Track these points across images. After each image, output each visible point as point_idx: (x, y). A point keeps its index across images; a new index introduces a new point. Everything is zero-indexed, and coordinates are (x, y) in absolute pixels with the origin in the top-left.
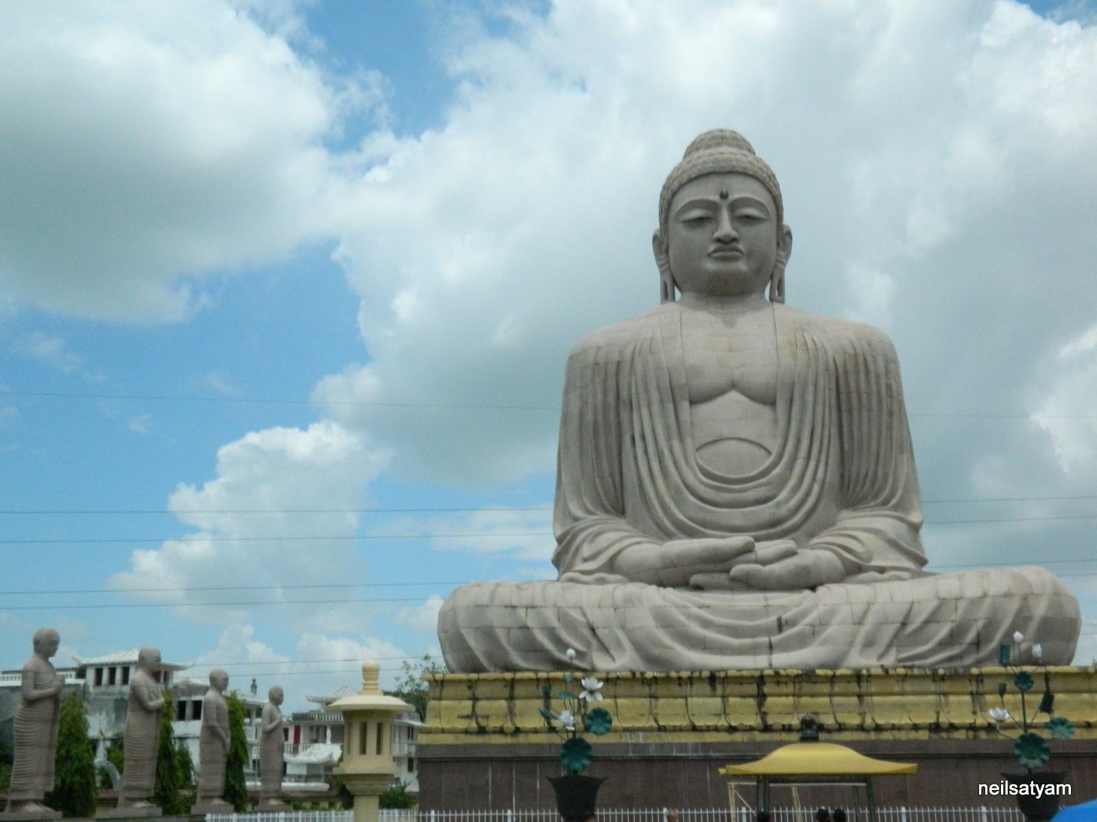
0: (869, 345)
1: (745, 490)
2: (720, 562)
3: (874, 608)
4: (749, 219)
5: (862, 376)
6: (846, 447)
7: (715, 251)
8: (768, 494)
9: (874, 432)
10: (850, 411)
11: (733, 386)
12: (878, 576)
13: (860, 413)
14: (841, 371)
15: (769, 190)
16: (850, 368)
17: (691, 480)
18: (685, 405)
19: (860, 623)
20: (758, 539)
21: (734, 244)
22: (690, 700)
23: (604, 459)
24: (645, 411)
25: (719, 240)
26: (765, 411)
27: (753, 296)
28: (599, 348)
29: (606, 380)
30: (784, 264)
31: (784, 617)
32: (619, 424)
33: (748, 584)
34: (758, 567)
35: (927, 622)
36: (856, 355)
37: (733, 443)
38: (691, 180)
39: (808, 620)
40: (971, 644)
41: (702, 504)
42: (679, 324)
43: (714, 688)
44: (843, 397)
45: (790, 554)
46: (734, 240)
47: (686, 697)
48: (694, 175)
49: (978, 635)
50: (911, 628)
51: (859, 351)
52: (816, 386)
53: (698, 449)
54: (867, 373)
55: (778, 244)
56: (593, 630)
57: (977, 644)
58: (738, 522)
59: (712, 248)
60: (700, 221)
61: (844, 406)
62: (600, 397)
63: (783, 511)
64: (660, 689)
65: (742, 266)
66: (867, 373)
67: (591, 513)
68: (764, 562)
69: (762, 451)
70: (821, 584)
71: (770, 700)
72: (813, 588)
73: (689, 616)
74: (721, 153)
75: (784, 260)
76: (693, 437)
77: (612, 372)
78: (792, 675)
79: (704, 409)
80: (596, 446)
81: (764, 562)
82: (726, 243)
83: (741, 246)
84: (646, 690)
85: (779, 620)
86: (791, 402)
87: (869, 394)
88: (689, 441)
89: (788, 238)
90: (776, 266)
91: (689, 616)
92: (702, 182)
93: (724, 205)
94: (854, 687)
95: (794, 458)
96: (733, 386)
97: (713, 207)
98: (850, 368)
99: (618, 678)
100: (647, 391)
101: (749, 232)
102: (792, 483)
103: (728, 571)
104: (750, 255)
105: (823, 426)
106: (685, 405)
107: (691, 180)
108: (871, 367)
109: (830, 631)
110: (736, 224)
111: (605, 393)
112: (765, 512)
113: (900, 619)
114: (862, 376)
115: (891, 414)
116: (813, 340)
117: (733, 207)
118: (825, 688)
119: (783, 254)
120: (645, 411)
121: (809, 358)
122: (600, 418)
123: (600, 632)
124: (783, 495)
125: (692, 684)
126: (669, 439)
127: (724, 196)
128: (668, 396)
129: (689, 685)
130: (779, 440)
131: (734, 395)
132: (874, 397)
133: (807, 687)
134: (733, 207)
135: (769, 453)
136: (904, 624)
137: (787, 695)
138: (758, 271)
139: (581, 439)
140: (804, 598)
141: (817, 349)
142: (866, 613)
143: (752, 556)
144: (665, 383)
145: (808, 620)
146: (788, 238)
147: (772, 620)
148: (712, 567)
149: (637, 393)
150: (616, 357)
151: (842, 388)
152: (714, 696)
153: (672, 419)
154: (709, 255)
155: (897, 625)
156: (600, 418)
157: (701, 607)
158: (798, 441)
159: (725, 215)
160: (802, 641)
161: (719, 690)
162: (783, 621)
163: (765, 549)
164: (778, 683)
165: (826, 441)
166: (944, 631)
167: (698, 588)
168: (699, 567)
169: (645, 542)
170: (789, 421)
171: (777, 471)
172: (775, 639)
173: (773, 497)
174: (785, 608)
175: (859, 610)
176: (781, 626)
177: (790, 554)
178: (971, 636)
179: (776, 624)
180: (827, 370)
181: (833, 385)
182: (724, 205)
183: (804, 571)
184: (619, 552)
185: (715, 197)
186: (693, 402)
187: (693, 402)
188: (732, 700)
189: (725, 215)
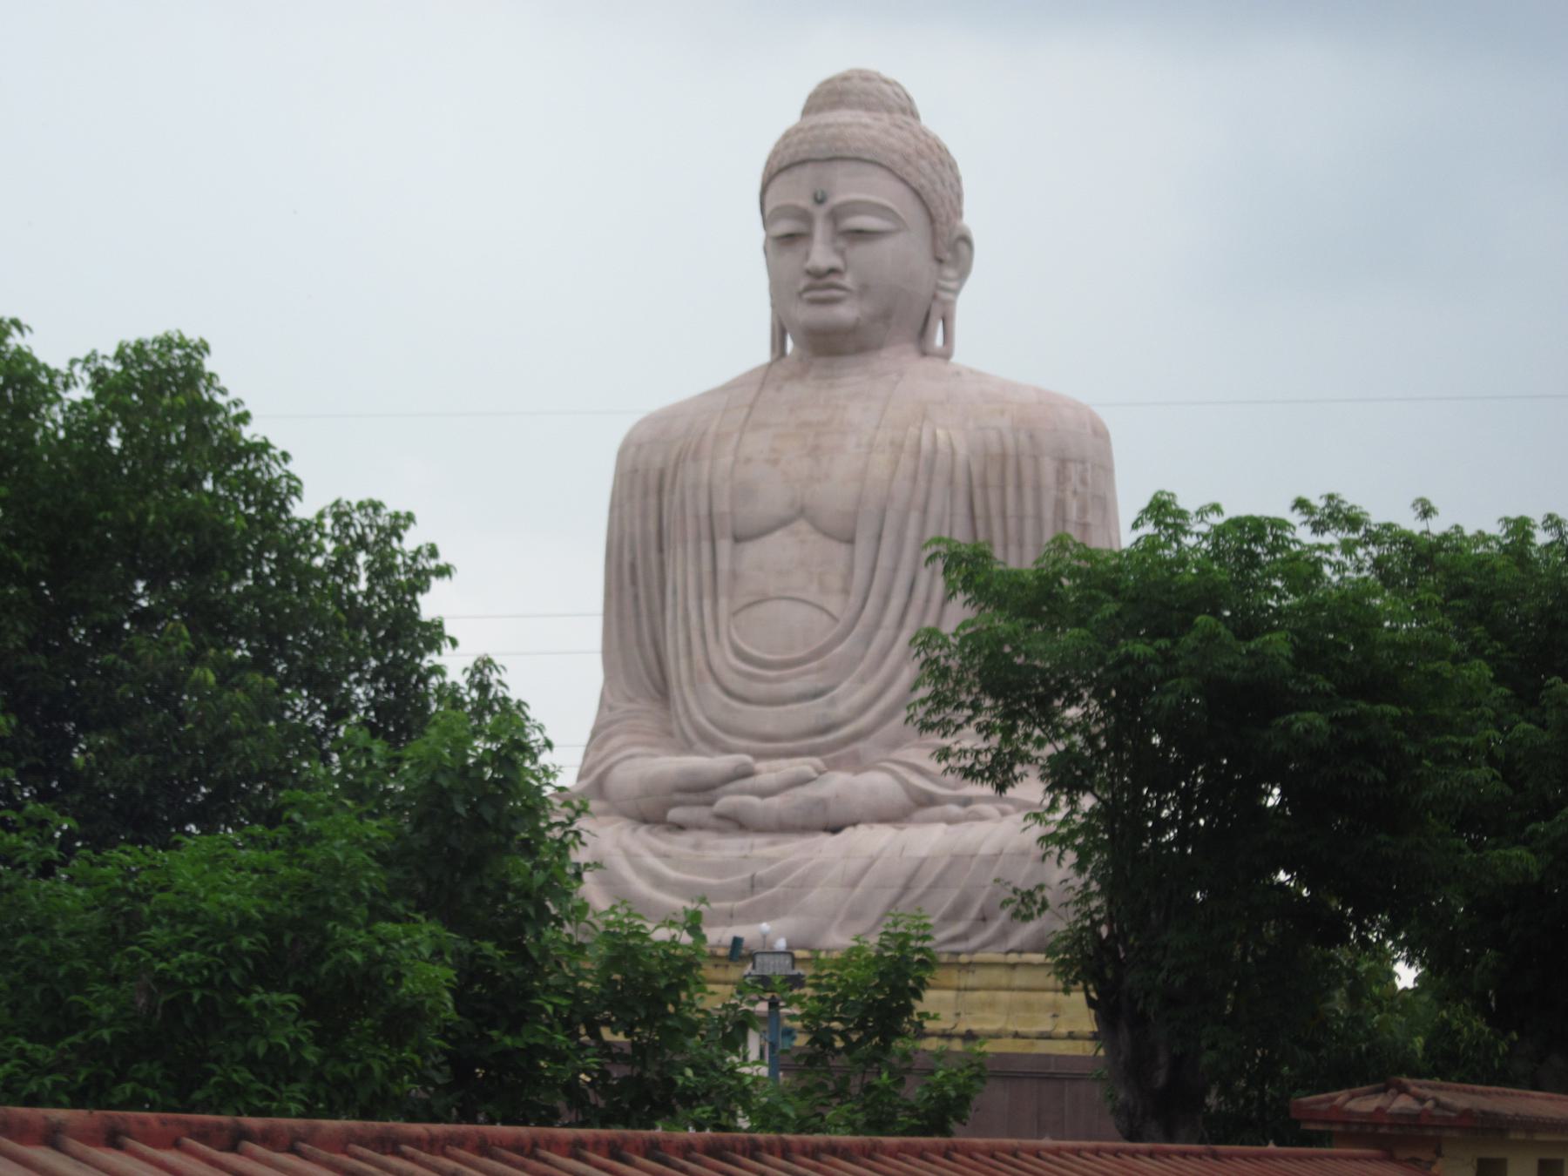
0: (1031, 437)
1: (779, 680)
2: (701, 789)
3: (878, 864)
5: (1011, 490)
7: (808, 289)
8: (821, 685)
12: (954, 809)
14: (976, 482)
15: (903, 181)
16: (993, 478)
17: (717, 662)
18: (724, 546)
19: (853, 884)
20: (759, 756)
21: (834, 279)
23: (644, 620)
24: (679, 550)
25: (808, 273)
26: (839, 551)
27: (884, 353)
28: (640, 446)
29: (645, 494)
30: (956, 292)
31: (762, 872)
33: (737, 823)
34: (755, 800)
35: (934, 886)
36: (1004, 456)
37: (784, 604)
38: (781, 170)
39: (785, 882)
40: (977, 920)
41: (726, 699)
42: (745, 410)
44: (980, 524)
45: (804, 781)
46: (833, 271)
48: (785, 163)
49: (982, 909)
50: (918, 892)
51: (1011, 451)
52: (925, 511)
53: (735, 614)
54: (1019, 487)
55: (940, 261)
57: (983, 919)
58: (769, 728)
59: (804, 282)
60: (789, 239)
62: (638, 523)
63: (841, 710)
65: (846, 313)
66: (1019, 487)
67: (630, 700)
68: (764, 793)
69: (825, 617)
70: (854, 824)
72: (835, 830)
73: (641, 870)
74: (828, 126)
75: (952, 285)
79: (752, 551)
80: (636, 597)
81: (764, 793)
82: (821, 277)
83: (848, 281)
86: (879, 537)
87: (1021, 519)
88: (723, 602)
89: (963, 247)
90: (935, 297)
91: (641, 870)
92: (797, 172)
93: (820, 212)
95: (877, 625)
96: (801, 512)
97: (805, 217)
98: (993, 478)
101: (861, 253)
102: (861, 668)
103: (710, 804)
104: (864, 290)
107: (781, 170)
108: (1028, 473)
109: (814, 896)
110: (841, 243)
111: (644, 517)
112: (810, 713)
113: (900, 881)
114: (1011, 490)
116: (935, 435)
117: (835, 216)
119: (950, 272)
120: (679, 550)
121: (893, 474)
122: (639, 556)
124: (845, 685)
126: (700, 598)
127: (819, 200)
128: (705, 531)
130: (854, 600)
131: (802, 526)
132: (1029, 525)
134: (835, 216)
135: (835, 619)
136: (907, 888)
137: (726, 983)
138: (885, 316)
139: (621, 588)
140: (827, 844)
141: (935, 450)
142: (864, 871)
143: (747, 783)
144: (703, 511)
145: (785, 882)
146: (963, 247)
147: (737, 879)
148: (693, 797)
150: (657, 461)
151: (979, 510)
153: (706, 566)
155: (895, 891)
156: (639, 556)
157: (664, 856)
158: (886, 598)
159: (821, 230)
160: (772, 910)
163: (770, 772)
166: (949, 898)
167: (680, 827)
168: (678, 797)
169: (642, 755)
170: (873, 570)
171: (839, 649)
173: (832, 688)
174: (770, 861)
175: (855, 865)
176: (754, 884)
177: (804, 781)
178: (974, 912)
180: (951, 482)
182: (820, 212)
183: (822, 803)
184: (610, 768)
185: (805, 202)
186: (738, 539)
187: (738, 539)
189: (821, 230)
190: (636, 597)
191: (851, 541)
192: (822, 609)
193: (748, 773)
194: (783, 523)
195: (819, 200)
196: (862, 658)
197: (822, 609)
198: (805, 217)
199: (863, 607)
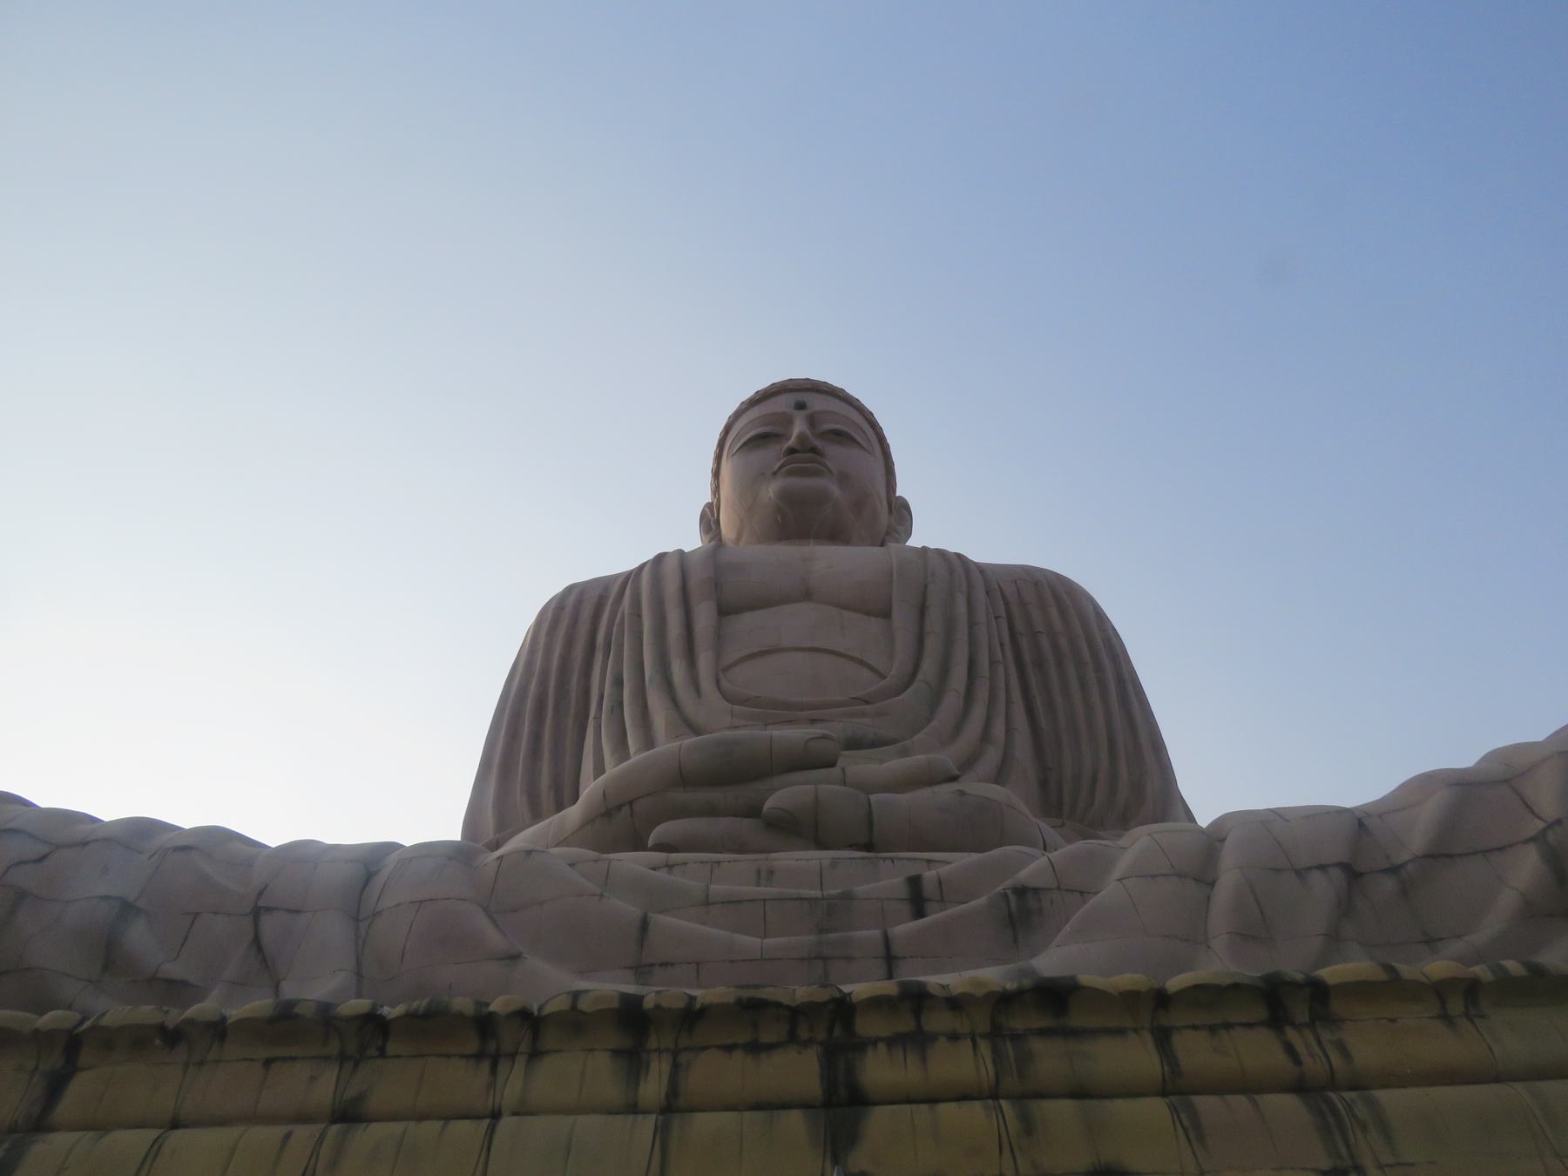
4: (839, 436)
6: (1044, 722)
7: (781, 467)
9: (1096, 698)
10: (1040, 665)
11: (807, 595)
13: (1060, 665)
22: (507, 1122)
25: (792, 451)
32: (586, 692)
35: (1439, 855)
43: (632, 1060)
44: (1025, 643)
46: (814, 450)
47: (496, 1115)
55: (890, 511)
56: (257, 913)
61: (1027, 657)
64: (390, 1081)
68: (868, 788)
71: (879, 1120)
76: (718, 652)
77: (586, 613)
78: (980, 993)
84: (324, 1087)
85: (915, 883)
86: (922, 610)
88: (704, 660)
94: (1257, 1050)
99: (218, 1029)
100: (638, 615)
105: (992, 663)
106: (704, 615)
115: (1121, 681)
118: (1134, 1056)
123: (268, 924)
125: (535, 1054)
129: (521, 1061)
133: (1050, 1059)
134: (812, 421)
149: (622, 623)
151: (1020, 625)
152: (633, 1109)
154: (775, 474)
161: (653, 1088)
162: (929, 888)
164: (919, 1041)
165: (1002, 685)
172: (904, 929)
176: (917, 899)
179: (903, 892)
181: (1003, 613)
187: (725, 611)
188: (704, 1123)
190: (536, 738)
191: (886, 614)
192: (861, 663)
193: (831, 764)
194: (786, 600)
195: (801, 406)
196: (929, 721)
197: (861, 663)
198: (788, 421)
199: (916, 667)
